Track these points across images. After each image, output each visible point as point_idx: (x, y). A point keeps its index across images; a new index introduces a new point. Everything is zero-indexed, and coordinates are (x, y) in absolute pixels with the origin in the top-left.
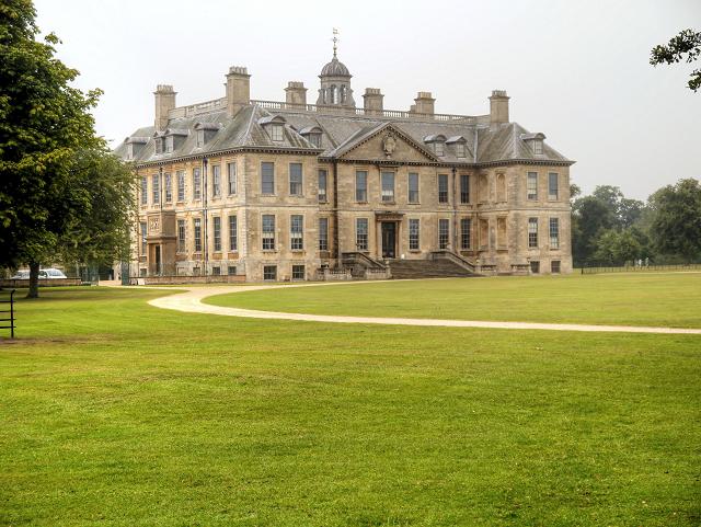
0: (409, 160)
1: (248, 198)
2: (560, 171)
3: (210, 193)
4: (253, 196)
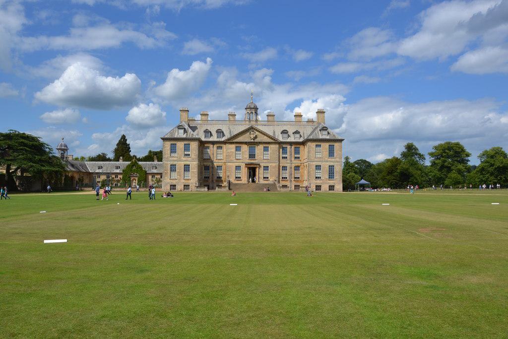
0: (264, 141)
2: (336, 145)
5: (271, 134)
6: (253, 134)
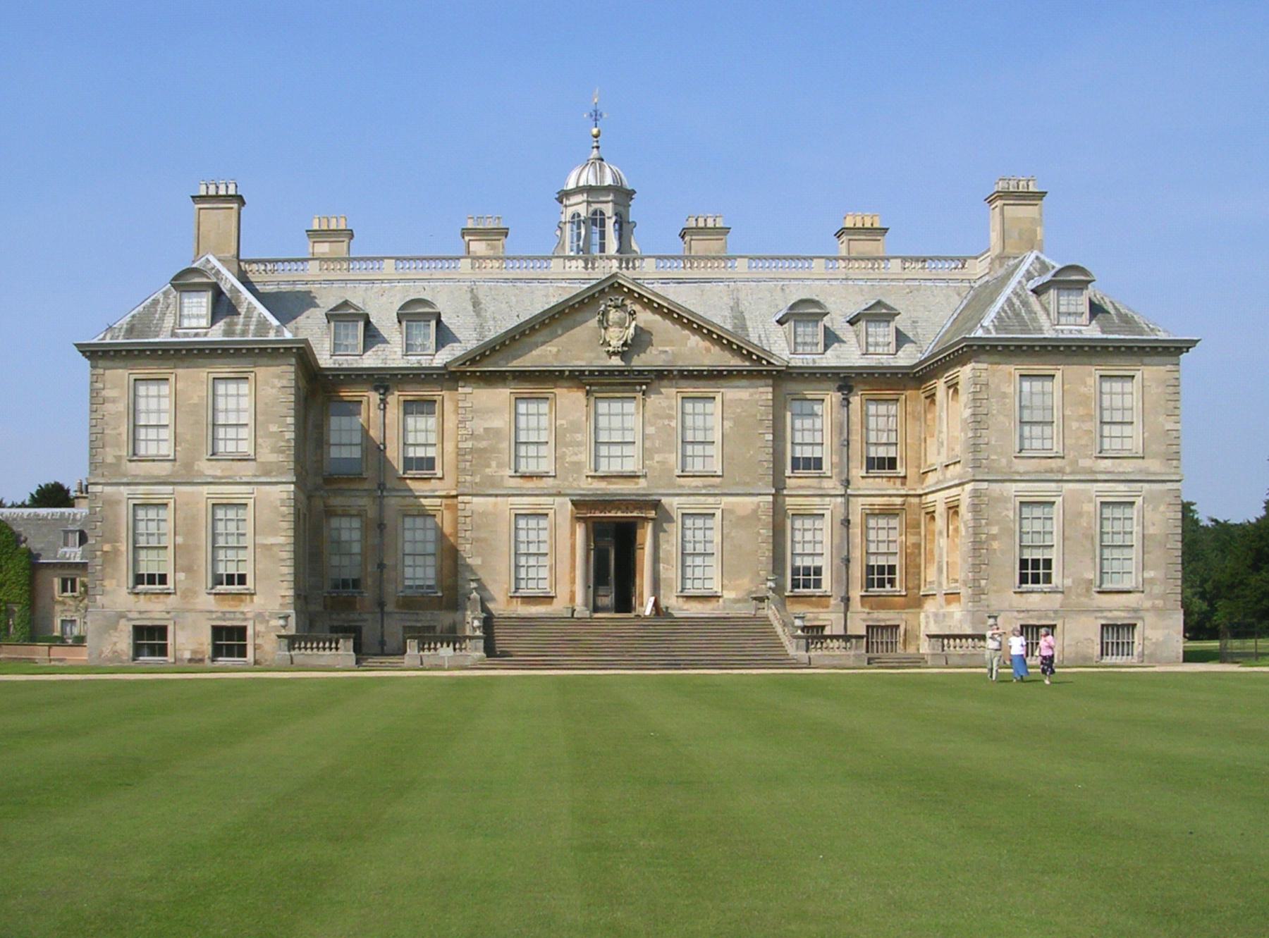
4: (110, 459)
5: (720, 318)
6: (621, 324)
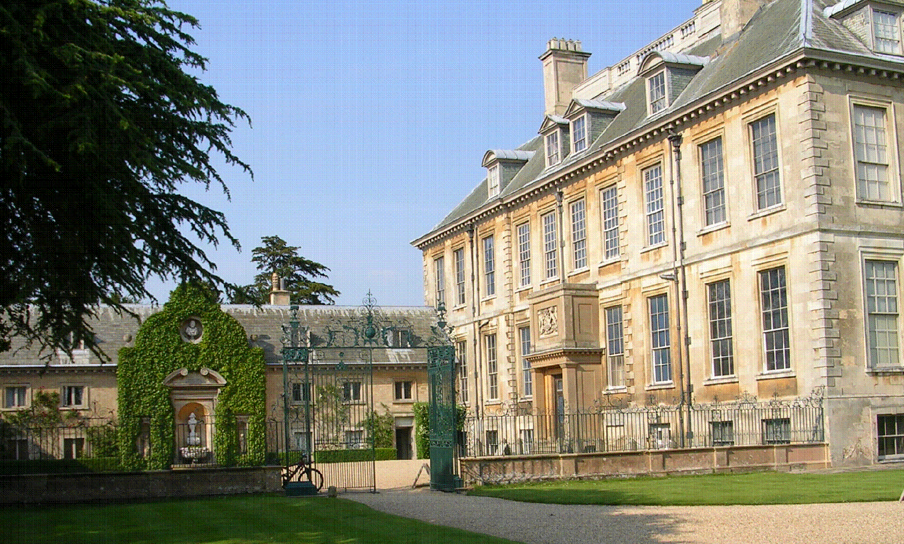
1: (824, 207)
3: (693, 219)
